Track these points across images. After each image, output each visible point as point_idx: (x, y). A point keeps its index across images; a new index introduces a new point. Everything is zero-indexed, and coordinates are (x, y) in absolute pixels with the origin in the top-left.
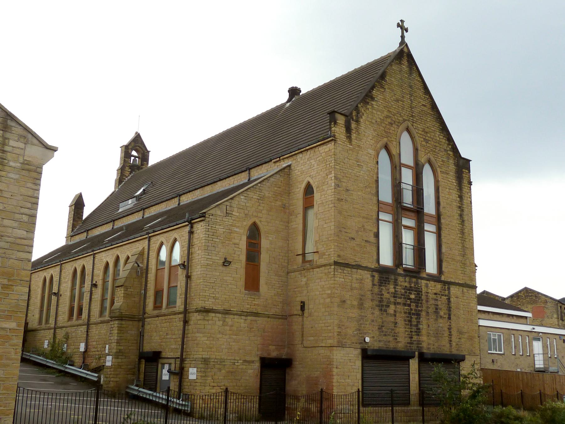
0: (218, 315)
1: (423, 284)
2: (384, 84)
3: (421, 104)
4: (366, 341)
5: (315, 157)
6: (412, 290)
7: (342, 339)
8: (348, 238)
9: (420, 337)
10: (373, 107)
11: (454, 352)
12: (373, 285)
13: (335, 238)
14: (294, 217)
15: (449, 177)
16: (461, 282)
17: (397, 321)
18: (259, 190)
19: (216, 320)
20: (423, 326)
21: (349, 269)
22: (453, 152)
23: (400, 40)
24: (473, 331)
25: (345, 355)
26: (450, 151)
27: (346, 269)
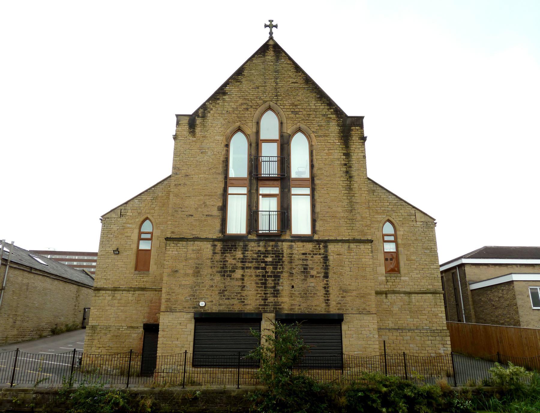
0: (108, 292)
3: (291, 83)
4: (204, 305)
6: (268, 254)
7: (172, 304)
8: (185, 216)
9: (279, 299)
12: (214, 253)
16: (347, 239)
17: (245, 285)
18: (153, 193)
19: (106, 296)
21: (185, 243)
24: (366, 288)
25: (173, 319)
27: (180, 242)
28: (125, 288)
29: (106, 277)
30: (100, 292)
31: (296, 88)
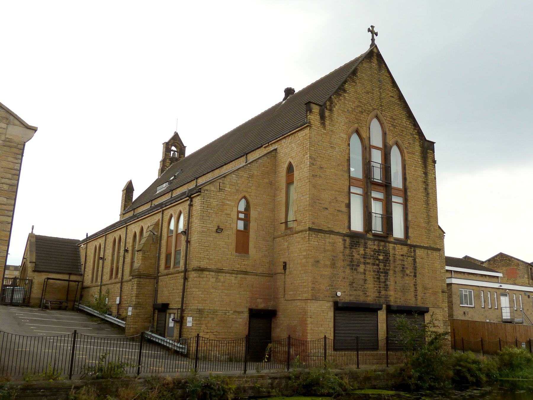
1: (391, 247)
2: (355, 79)
5: (295, 141)
6: (381, 252)
9: (388, 292)
10: (345, 98)
11: (420, 304)
12: (345, 247)
13: (310, 208)
14: (279, 192)
15: (414, 156)
16: (426, 246)
17: (366, 278)
20: (391, 283)
21: (322, 234)
22: (419, 135)
26: (416, 135)
27: (320, 234)
28: (228, 270)
29: (208, 257)
30: (204, 272)
31: (393, 103)
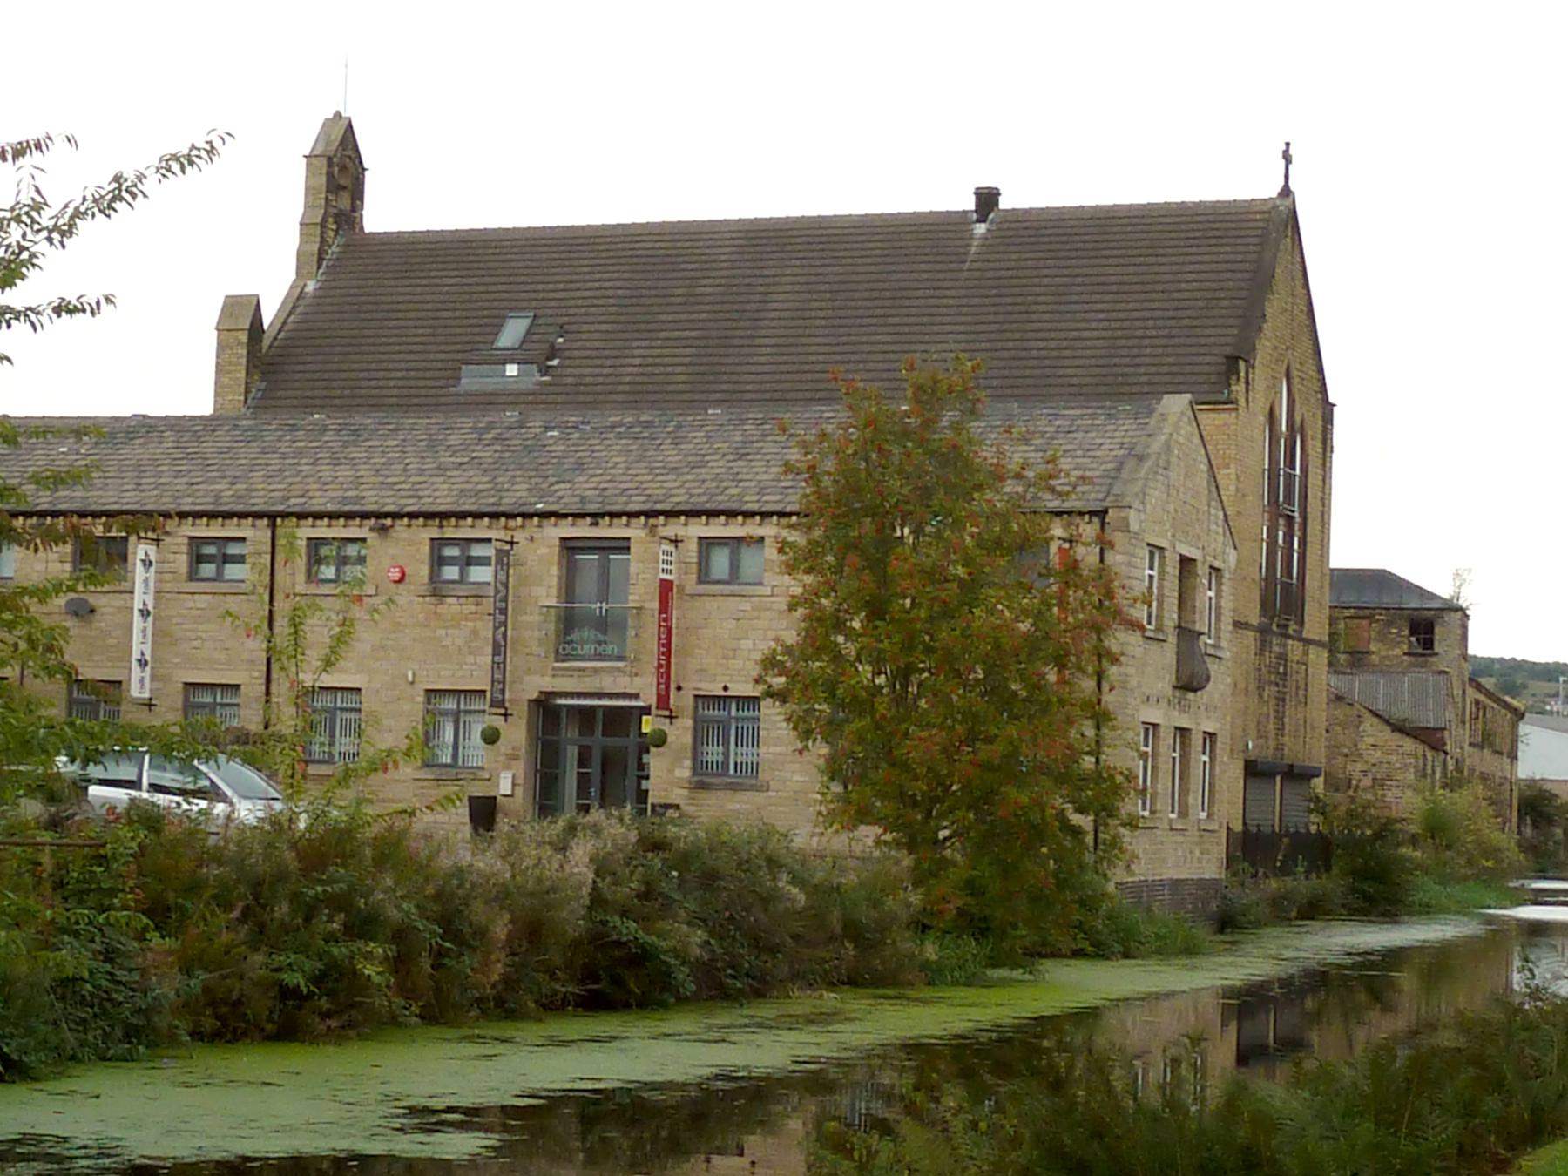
23: (1282, 183)
